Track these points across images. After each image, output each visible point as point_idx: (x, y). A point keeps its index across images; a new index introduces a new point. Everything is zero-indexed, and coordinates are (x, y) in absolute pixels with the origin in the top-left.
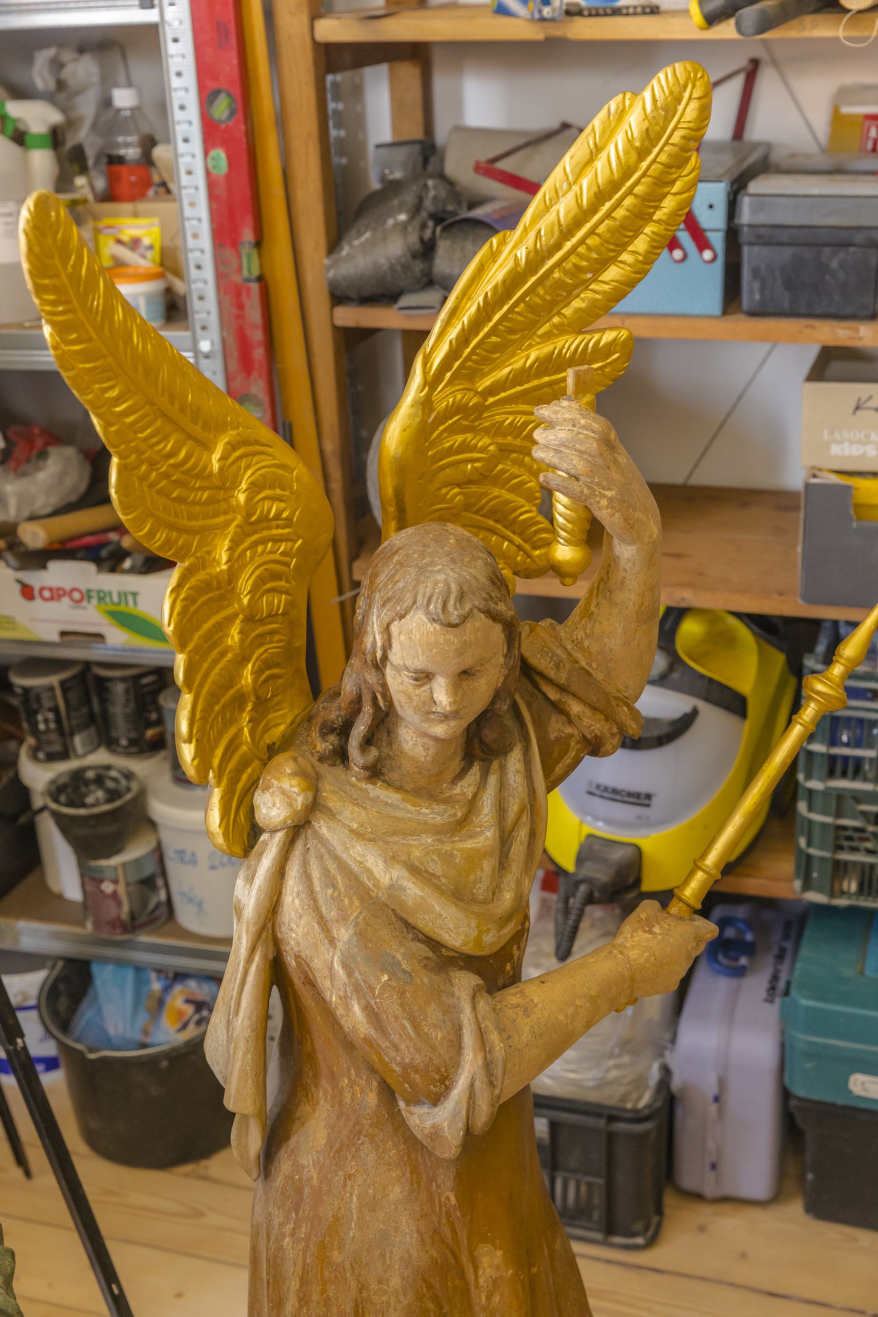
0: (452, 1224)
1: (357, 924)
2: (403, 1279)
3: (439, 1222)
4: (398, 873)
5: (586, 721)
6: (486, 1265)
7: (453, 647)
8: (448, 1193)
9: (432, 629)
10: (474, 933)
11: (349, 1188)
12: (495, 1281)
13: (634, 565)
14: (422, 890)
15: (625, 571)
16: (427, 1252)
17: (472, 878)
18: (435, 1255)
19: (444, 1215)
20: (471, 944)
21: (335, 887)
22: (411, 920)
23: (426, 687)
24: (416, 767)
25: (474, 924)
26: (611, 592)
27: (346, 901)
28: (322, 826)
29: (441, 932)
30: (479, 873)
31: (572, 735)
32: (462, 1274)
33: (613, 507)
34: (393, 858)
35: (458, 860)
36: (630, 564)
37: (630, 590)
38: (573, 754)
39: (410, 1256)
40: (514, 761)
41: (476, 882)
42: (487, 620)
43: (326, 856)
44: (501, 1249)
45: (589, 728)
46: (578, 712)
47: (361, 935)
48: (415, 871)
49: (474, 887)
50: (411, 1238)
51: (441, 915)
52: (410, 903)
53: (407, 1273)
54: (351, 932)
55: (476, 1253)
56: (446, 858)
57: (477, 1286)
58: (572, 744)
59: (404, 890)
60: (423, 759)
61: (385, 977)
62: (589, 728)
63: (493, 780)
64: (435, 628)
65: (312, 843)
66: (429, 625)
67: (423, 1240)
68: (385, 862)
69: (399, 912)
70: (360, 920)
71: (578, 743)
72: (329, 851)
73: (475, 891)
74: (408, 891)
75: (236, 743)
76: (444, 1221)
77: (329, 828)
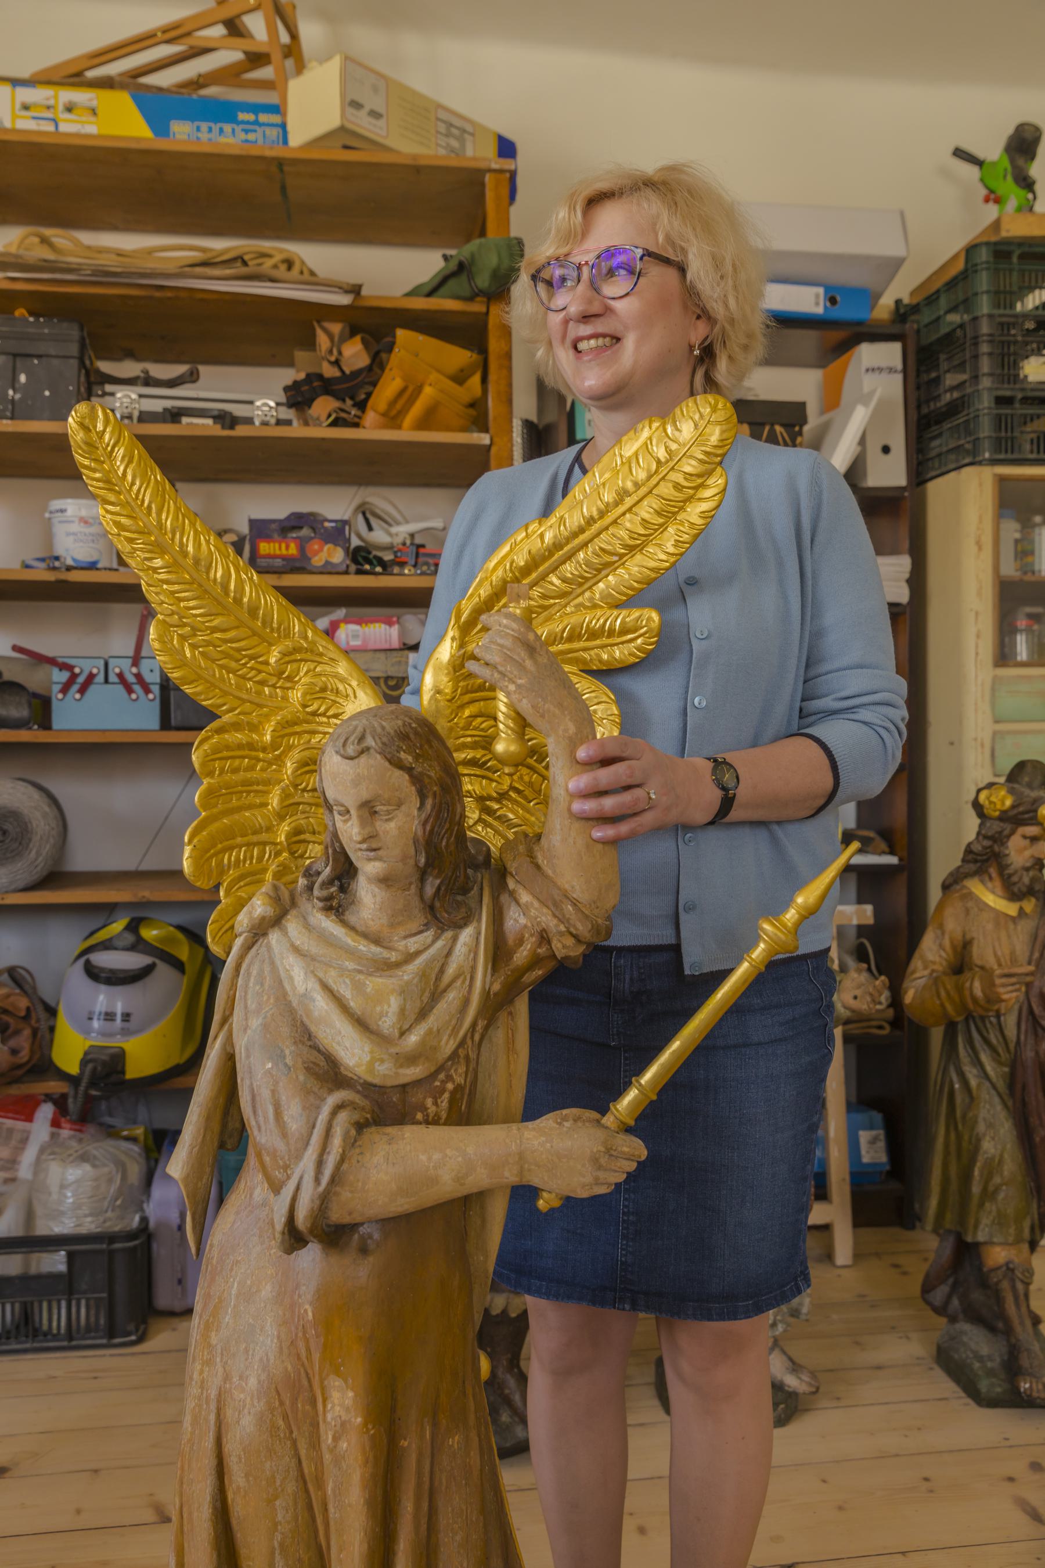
0: (307, 1341)
1: (265, 1017)
2: (259, 1382)
3: (296, 1335)
4: (312, 985)
6: (336, 1401)
8: (307, 1307)
10: (367, 1058)
11: (233, 1273)
12: (343, 1424)
14: (327, 1005)
16: (283, 1361)
17: (378, 1009)
18: (289, 1367)
19: (300, 1328)
20: (364, 1068)
21: (262, 985)
22: (313, 1028)
25: (367, 1049)
27: (265, 998)
28: (274, 937)
29: (338, 1048)
30: (386, 1007)
32: (313, 1402)
33: (520, 693)
34: (313, 972)
35: (369, 990)
39: (268, 1360)
40: (466, 935)
41: (381, 1015)
43: (267, 961)
44: (352, 1389)
47: (265, 1026)
48: (326, 987)
49: (380, 1019)
50: (272, 1341)
51: (340, 1033)
52: (316, 1014)
53: (263, 1377)
54: (260, 1021)
55: (326, 1383)
56: (358, 987)
57: (325, 1421)
59: (314, 1001)
61: (270, 1065)
65: (263, 949)
67: (281, 1348)
68: (306, 974)
69: (305, 1019)
70: (268, 1015)
72: (270, 957)
73: (380, 1023)
74: (317, 1003)
76: (300, 1334)
77: (277, 940)
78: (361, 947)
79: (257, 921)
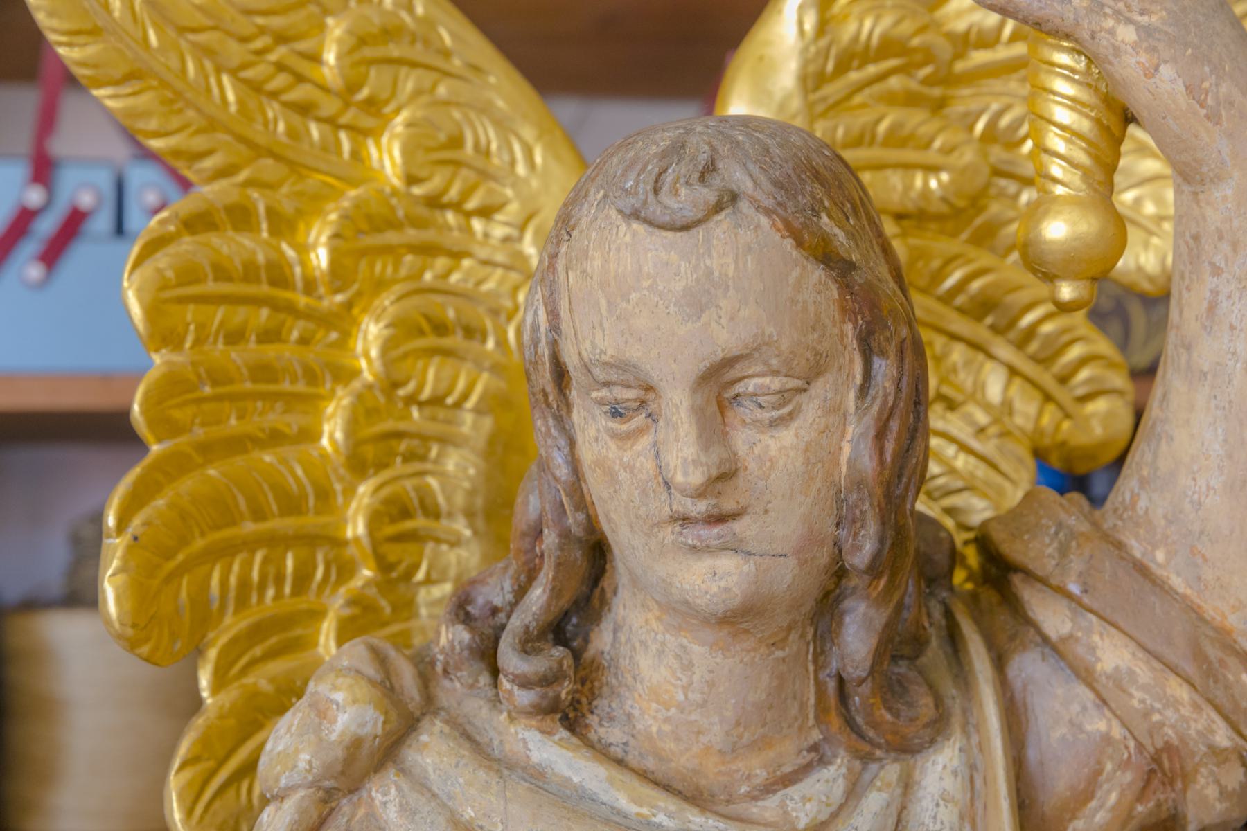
5: (1137, 698)
7: (679, 286)
9: (628, 238)
13: (1235, 246)
15: (1216, 271)
23: (644, 442)
24: (667, 720)
26: (1188, 348)
31: (1107, 739)
33: (1153, 50)
36: (1225, 247)
37: (1232, 328)
38: (1113, 797)
40: (940, 770)
42: (777, 237)
45: (1146, 714)
46: (1117, 669)
58: (1109, 766)
60: (681, 697)
62: (1146, 714)
63: (874, 801)
64: (634, 235)
66: (623, 228)
71: (1125, 765)
75: (298, 632)
78: (660, 818)
79: (340, 753)
